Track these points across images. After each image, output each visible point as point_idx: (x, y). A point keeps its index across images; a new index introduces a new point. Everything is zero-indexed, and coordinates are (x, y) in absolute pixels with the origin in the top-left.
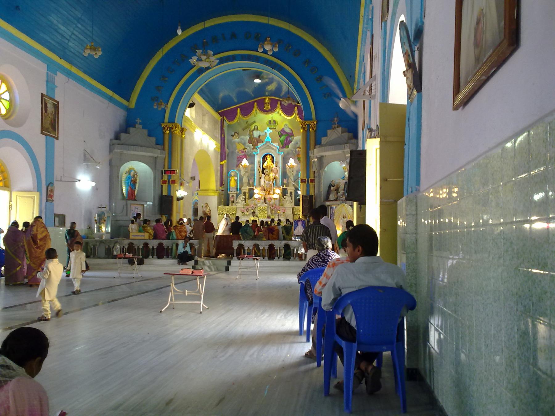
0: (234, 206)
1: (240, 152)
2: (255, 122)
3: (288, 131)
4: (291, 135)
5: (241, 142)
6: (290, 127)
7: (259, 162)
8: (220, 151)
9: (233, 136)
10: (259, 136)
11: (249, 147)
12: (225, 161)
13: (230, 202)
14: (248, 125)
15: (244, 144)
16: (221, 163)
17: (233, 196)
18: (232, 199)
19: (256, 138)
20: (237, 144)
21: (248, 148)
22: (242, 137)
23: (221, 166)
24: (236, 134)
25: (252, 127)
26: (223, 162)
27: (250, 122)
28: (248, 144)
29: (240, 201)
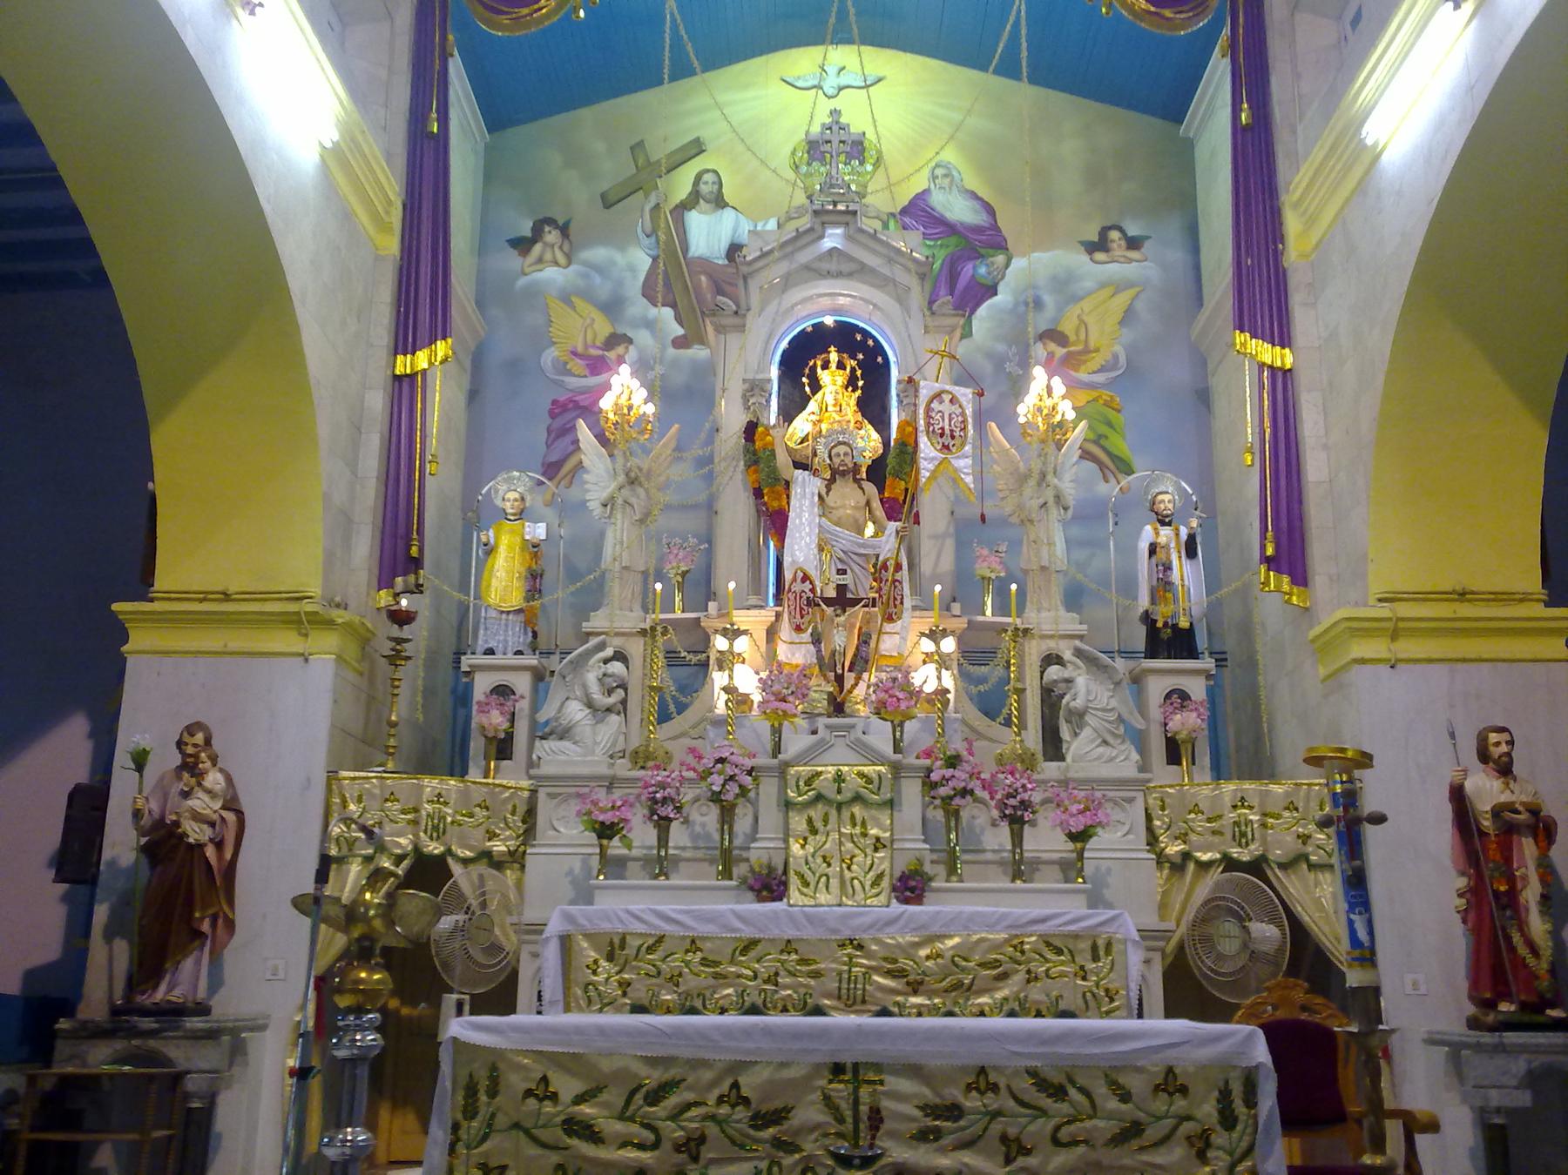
0: (512, 778)
1: (577, 366)
2: (697, 148)
3: (959, 210)
4: (987, 239)
5: (588, 295)
6: (972, 182)
7: (755, 388)
8: (391, 245)
9: (522, 245)
10: (734, 250)
11: (650, 325)
12: (442, 348)
13: (476, 745)
14: (646, 173)
15: (612, 307)
16: (403, 365)
17: (503, 691)
18: (496, 720)
19: (704, 264)
20: (557, 308)
21: (643, 337)
22: (598, 254)
23: (405, 388)
24: (552, 236)
25: (681, 184)
26: (422, 359)
27: (658, 153)
28: (639, 306)
29: (576, 711)
